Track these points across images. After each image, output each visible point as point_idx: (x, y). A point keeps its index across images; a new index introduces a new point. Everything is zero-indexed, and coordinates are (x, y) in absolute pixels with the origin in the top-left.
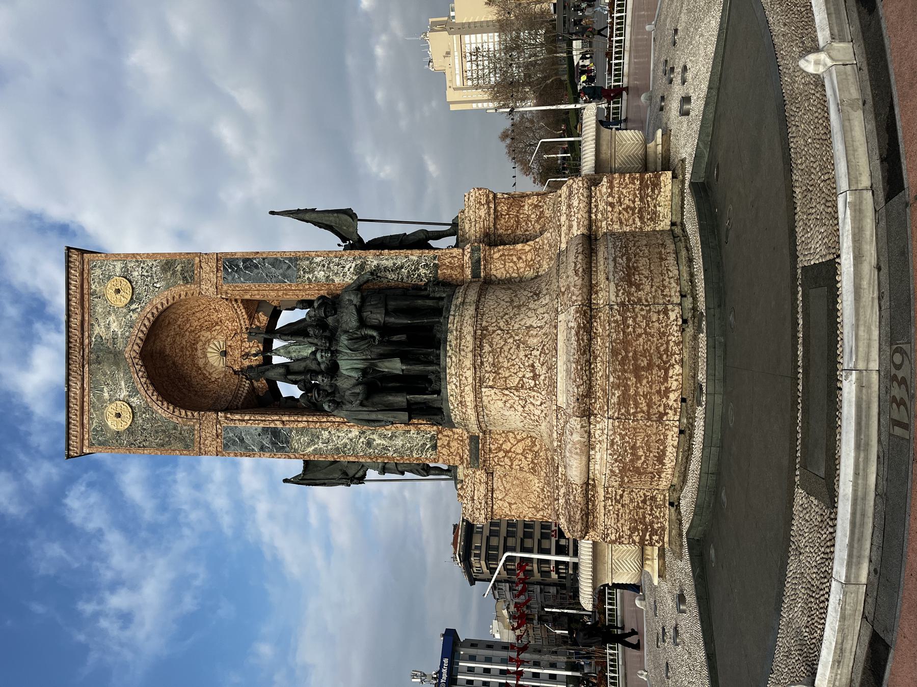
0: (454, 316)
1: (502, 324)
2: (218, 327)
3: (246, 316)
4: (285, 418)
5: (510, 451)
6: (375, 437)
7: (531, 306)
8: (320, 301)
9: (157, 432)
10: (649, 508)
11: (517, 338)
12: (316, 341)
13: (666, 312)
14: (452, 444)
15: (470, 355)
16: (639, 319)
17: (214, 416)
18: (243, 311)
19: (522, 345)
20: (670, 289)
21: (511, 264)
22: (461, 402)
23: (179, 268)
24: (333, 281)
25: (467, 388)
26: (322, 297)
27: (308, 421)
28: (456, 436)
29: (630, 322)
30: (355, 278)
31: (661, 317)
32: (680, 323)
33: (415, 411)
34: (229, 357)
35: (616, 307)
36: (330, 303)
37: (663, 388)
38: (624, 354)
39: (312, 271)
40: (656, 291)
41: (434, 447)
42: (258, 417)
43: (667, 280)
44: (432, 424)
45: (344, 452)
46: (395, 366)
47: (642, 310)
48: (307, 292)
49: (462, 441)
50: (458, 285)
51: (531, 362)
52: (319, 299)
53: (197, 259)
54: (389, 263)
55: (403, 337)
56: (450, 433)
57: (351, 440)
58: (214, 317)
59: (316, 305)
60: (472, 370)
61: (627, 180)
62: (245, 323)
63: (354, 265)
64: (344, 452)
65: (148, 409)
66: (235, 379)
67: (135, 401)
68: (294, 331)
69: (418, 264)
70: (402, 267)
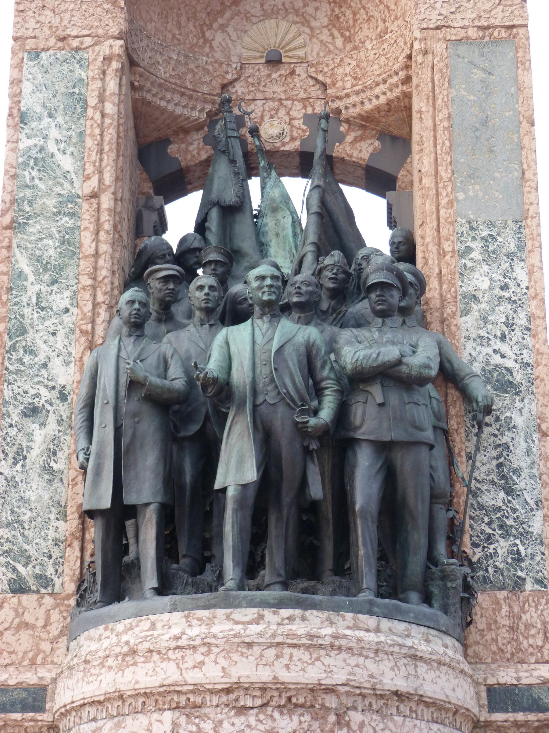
0: (377, 630)
2: (339, 42)
3: (368, 106)
4: (106, 201)
6: (52, 426)
8: (410, 277)
12: (306, 273)
14: (25, 634)
15: (264, 675)
17: (114, 30)
18: (383, 100)
22: (134, 652)
24: (466, 312)
25: (172, 666)
26: (421, 284)
27: (96, 255)
28: (46, 646)
30: (477, 368)
34: (264, 71)
36: (400, 292)
39: (490, 257)
41: (18, 588)
42: (111, 134)
44: (81, 581)
45: (13, 348)
46: (237, 467)
48: (433, 249)
49: (33, 662)
50: (465, 647)
52: (417, 275)
54: (519, 458)
55: (316, 490)
56: (54, 630)
58: (366, 31)
59: (402, 266)
60: (223, 682)
62: (355, 105)
63: (510, 364)
64: (13, 348)
66: (210, 86)
68: (334, 227)
69: (523, 536)
70: (509, 491)
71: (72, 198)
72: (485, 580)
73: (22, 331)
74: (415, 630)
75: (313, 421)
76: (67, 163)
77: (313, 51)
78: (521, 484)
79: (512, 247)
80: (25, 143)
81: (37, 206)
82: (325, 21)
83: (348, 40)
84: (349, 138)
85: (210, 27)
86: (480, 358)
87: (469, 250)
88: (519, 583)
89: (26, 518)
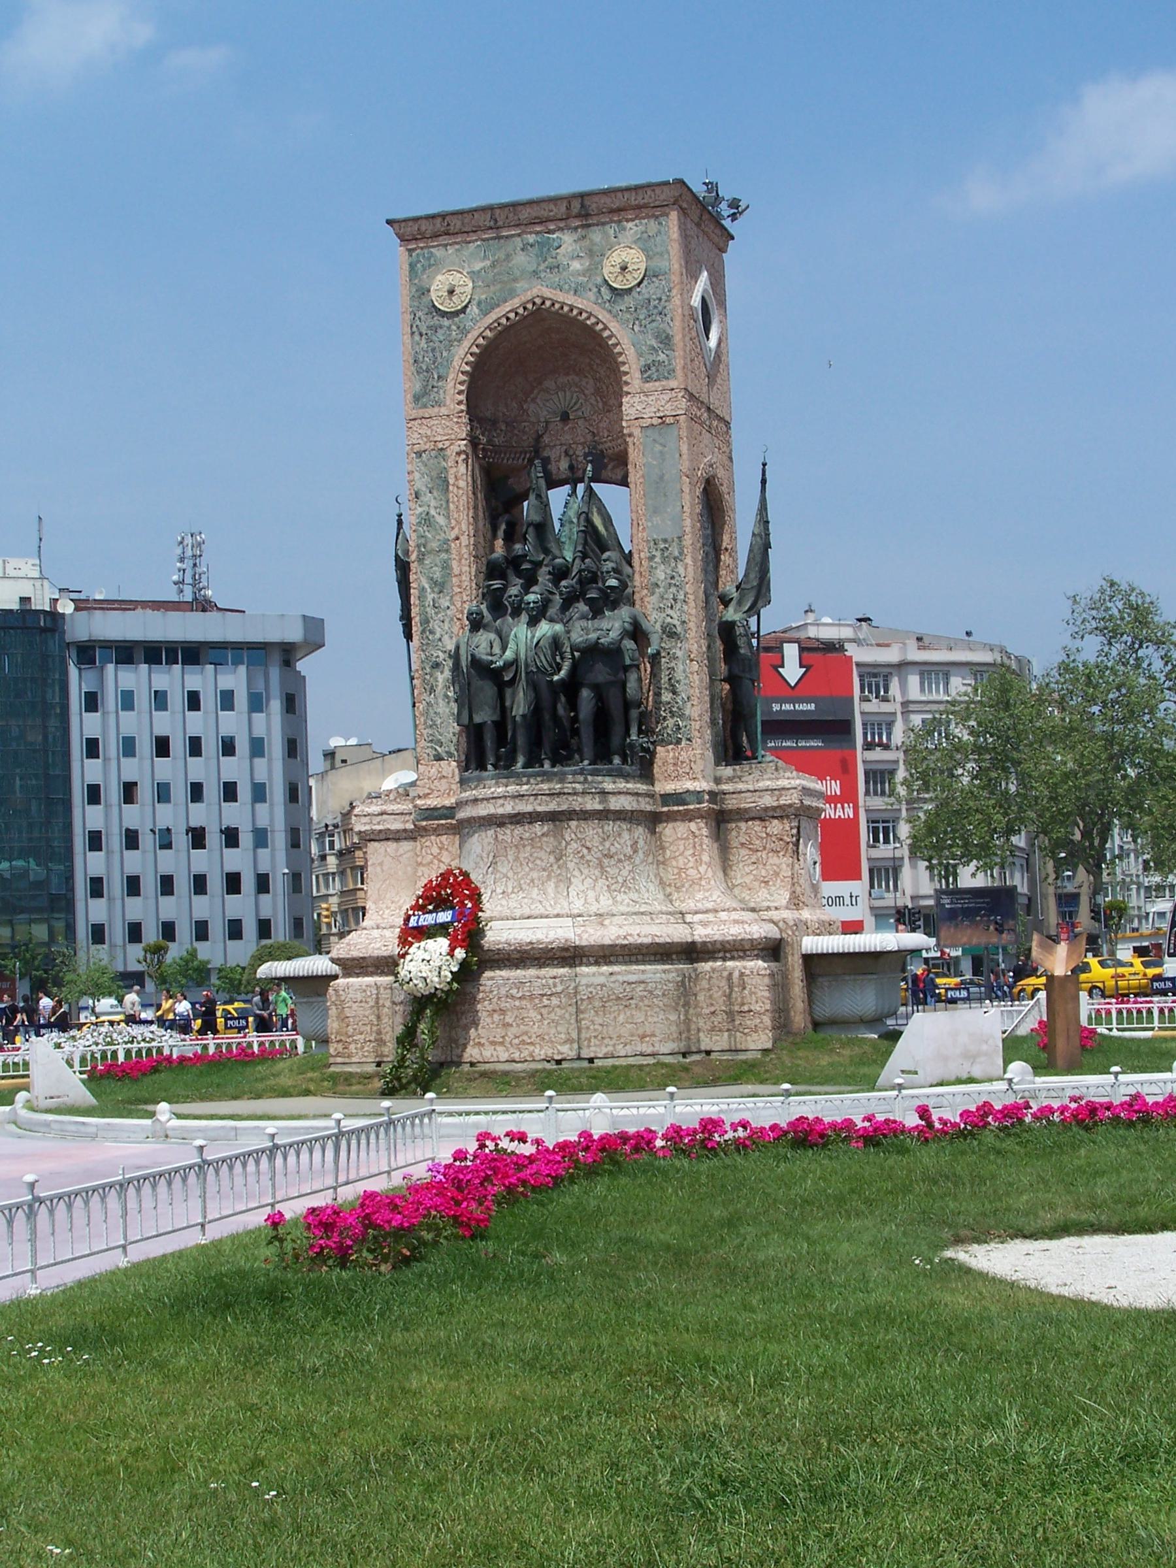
1: (574, 845)
2: (600, 405)
4: (464, 540)
5: (440, 861)
7: (601, 882)
9: (433, 350)
10: (372, 1038)
11: (555, 867)
13: (569, 1041)
15: (529, 808)
16: (559, 1012)
19: (545, 874)
20: (599, 1046)
21: (682, 848)
23: (662, 357)
24: (653, 594)
29: (555, 1001)
31: (563, 1036)
32: (557, 1057)
33: (474, 735)
34: (560, 425)
35: (573, 985)
37: (482, 1041)
38: (520, 995)
40: (595, 1030)
41: (439, 758)
43: (611, 1043)
47: (571, 1015)
51: (524, 886)
53: (673, 384)
54: (679, 675)
57: (440, 640)
61: (760, 994)
63: (677, 623)
65: (464, 332)
67: (474, 310)
69: (682, 716)
70: (674, 693)
71: (446, 541)
72: (663, 740)
73: (428, 622)
74: (607, 779)
75: (556, 678)
76: (441, 520)
77: (587, 410)
78: (679, 688)
79: (676, 554)
80: (420, 510)
81: (429, 548)
82: (592, 391)
83: (605, 403)
84: (610, 467)
85: (526, 401)
86: (660, 620)
87: (654, 556)
88: (679, 741)
89: (439, 722)
